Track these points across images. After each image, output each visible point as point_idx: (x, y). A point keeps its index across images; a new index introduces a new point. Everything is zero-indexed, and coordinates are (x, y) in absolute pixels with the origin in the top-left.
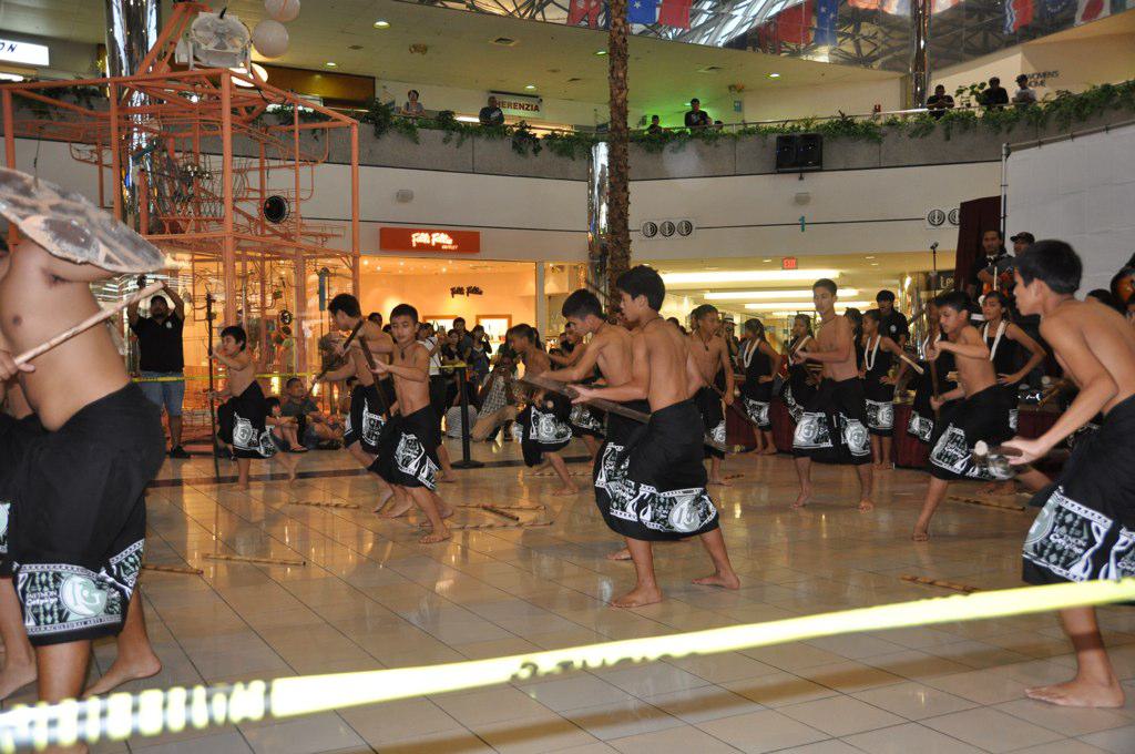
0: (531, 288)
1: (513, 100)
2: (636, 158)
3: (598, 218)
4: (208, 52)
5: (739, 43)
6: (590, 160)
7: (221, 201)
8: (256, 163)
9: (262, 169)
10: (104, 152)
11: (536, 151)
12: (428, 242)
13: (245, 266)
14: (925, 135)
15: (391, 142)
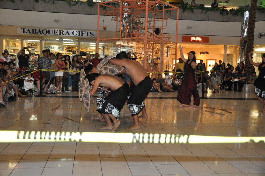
0: (223, 52)
2: (258, 15)
3: (244, 32)
6: (243, 16)
7: (144, 29)
8: (153, 20)
9: (154, 21)
10: (118, 18)
11: (227, 14)
12: (195, 40)
13: (149, 45)
15: (187, 13)
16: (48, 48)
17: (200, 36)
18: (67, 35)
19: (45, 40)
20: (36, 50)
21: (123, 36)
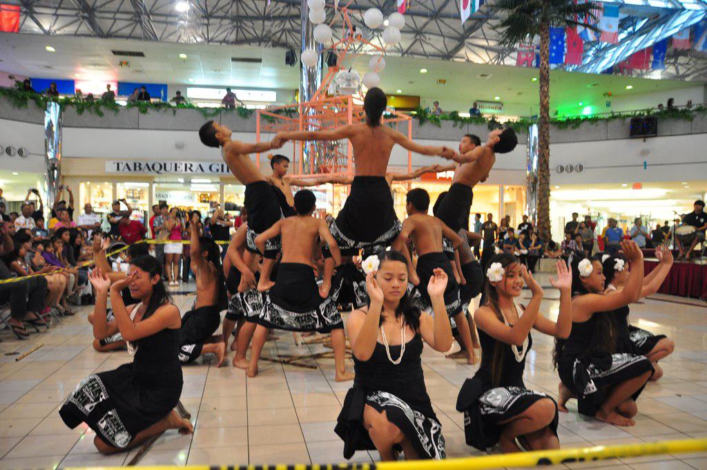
0: (496, 199)
1: (488, 105)
2: (553, 132)
3: (532, 163)
4: (342, 88)
5: (609, 71)
6: (528, 133)
7: (347, 157)
15: (427, 128)
16: (163, 197)
18: (200, 171)
19: (159, 183)
20: (140, 201)
21: (306, 170)
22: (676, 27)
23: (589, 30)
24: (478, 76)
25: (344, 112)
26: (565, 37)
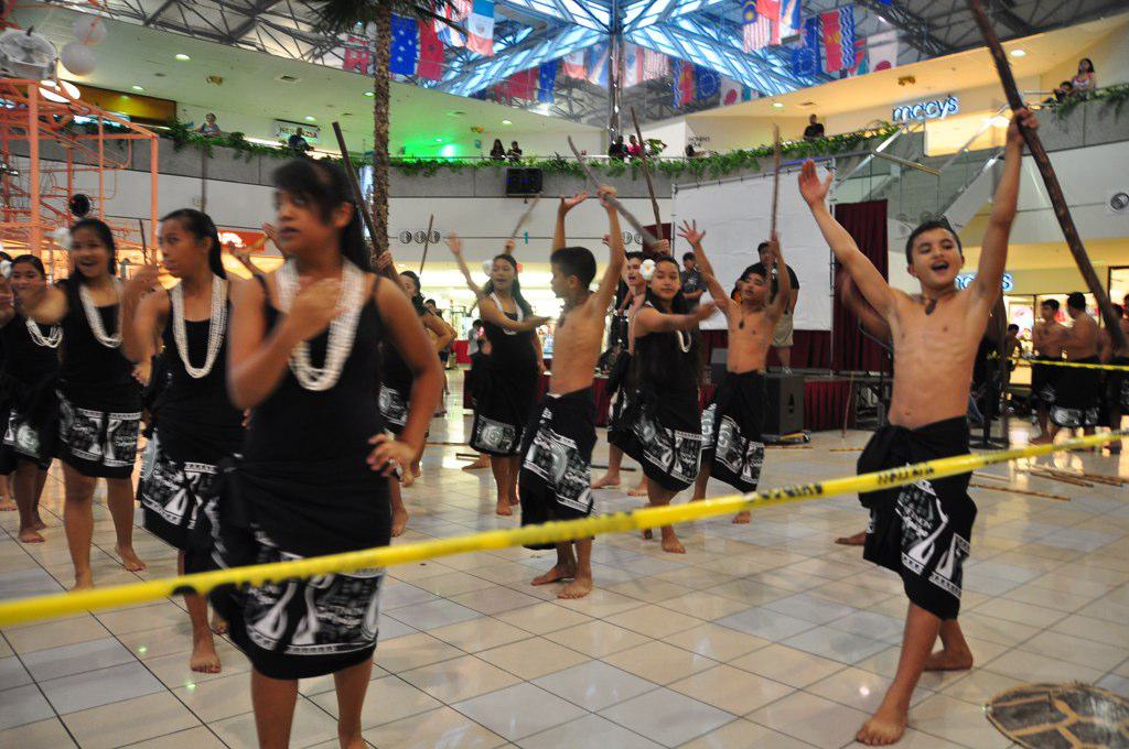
2: (394, 180)
5: (481, 95)
7: (29, 196)
8: (63, 166)
14: (618, 175)
15: (189, 157)
17: (236, 230)
22: (567, 46)
23: (452, 31)
24: (278, 79)
25: (22, 110)
26: (418, 36)
